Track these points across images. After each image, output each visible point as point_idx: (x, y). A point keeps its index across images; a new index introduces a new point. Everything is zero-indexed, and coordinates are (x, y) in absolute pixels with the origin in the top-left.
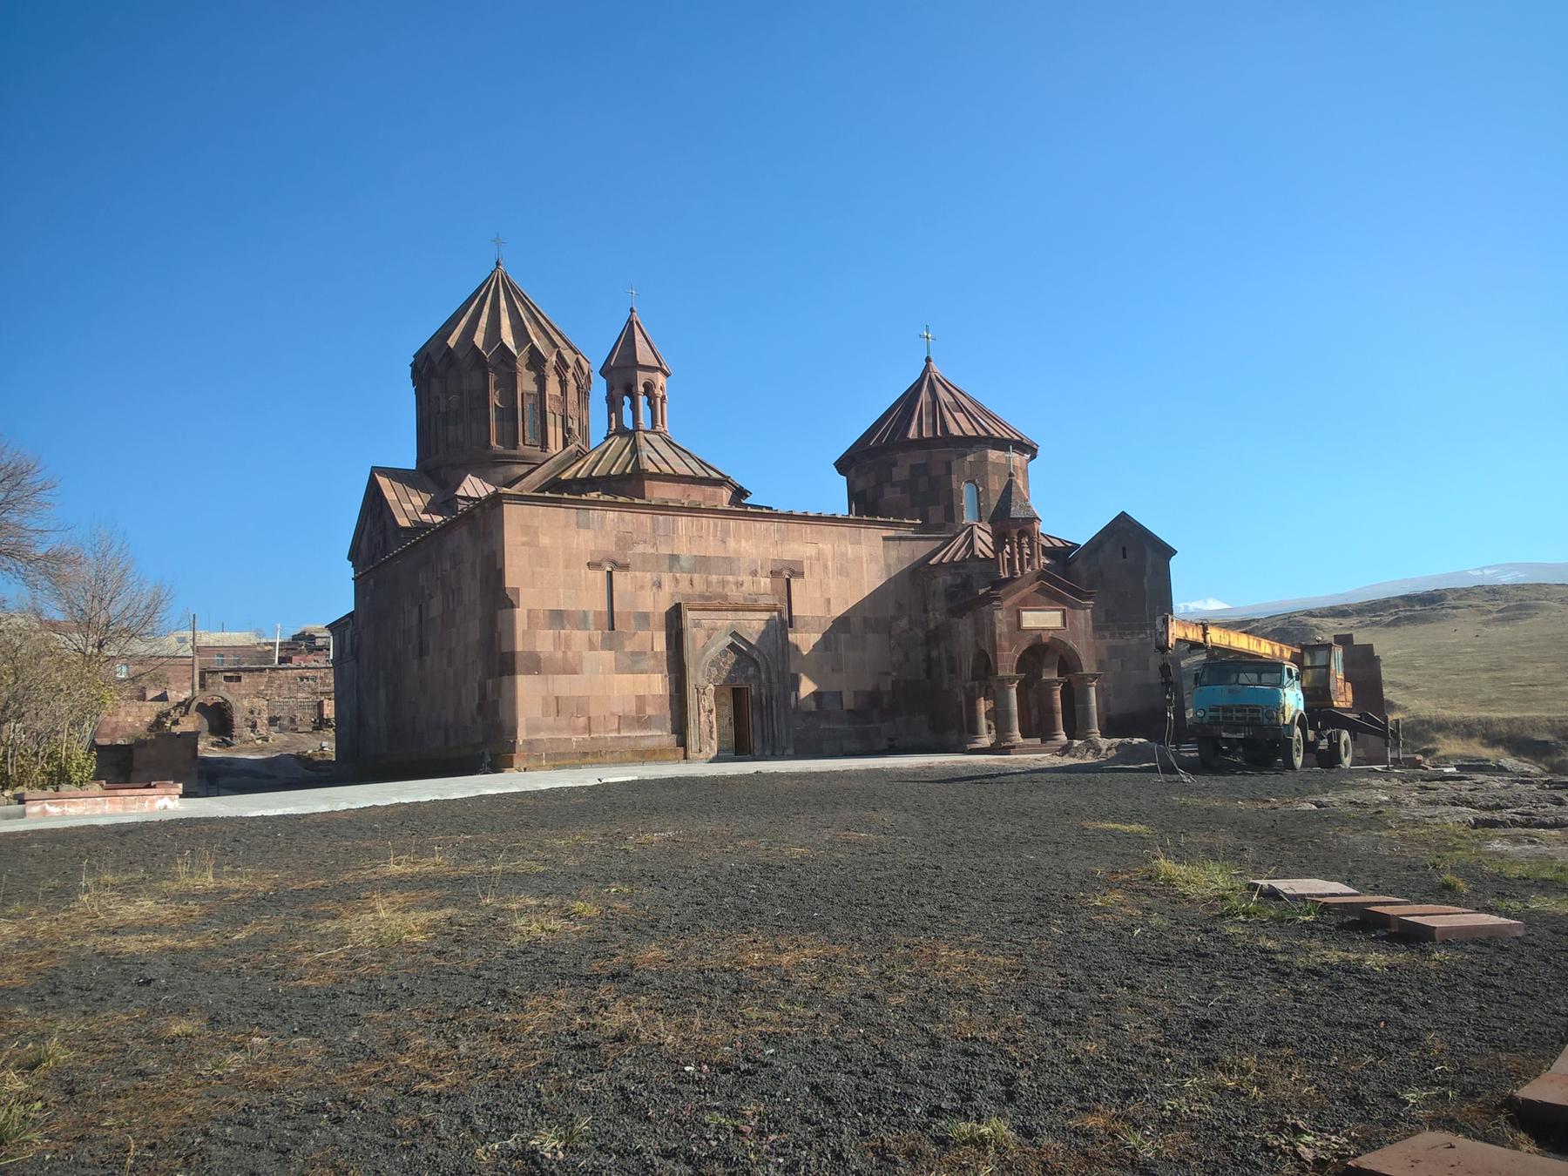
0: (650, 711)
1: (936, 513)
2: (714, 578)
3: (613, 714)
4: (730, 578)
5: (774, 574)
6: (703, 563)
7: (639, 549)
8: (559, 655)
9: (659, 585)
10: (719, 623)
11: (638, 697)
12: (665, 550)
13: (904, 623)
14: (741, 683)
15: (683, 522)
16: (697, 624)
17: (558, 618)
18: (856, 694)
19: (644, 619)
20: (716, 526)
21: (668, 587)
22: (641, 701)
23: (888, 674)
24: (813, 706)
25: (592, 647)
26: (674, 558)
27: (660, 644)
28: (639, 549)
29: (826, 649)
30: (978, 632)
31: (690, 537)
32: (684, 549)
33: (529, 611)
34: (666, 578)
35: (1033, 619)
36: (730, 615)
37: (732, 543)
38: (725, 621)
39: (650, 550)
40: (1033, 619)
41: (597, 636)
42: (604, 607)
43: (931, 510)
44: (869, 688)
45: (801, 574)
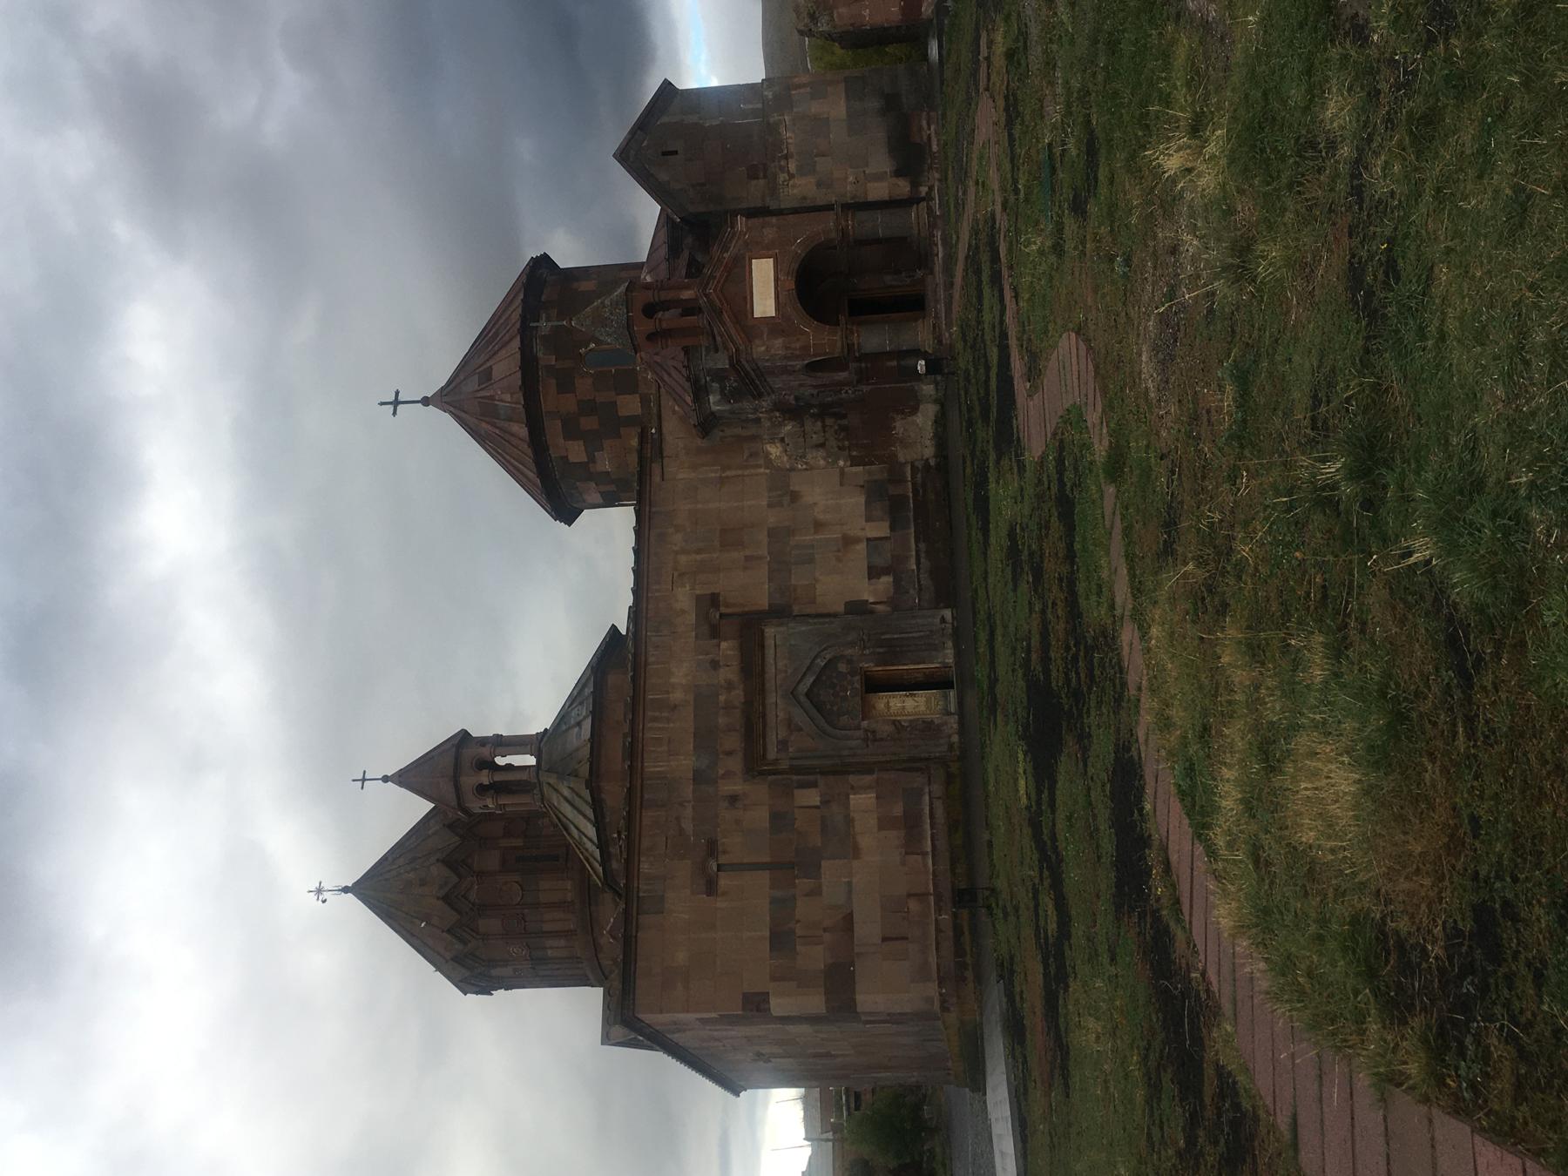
0: (898, 810)
1: (630, 405)
2: (722, 721)
3: (903, 863)
4: (722, 698)
5: (715, 633)
6: (705, 738)
7: (688, 826)
8: (827, 937)
9: (733, 799)
10: (781, 715)
11: (881, 828)
12: (688, 791)
13: (774, 451)
14: (857, 682)
15: (651, 767)
16: (783, 745)
17: (781, 940)
18: (868, 519)
19: (779, 820)
20: (655, 719)
21: (736, 786)
22: (885, 823)
23: (842, 473)
24: (886, 580)
25: (816, 892)
26: (699, 777)
27: (811, 797)
28: (688, 826)
29: (811, 560)
30: (785, 370)
31: (673, 758)
32: (684, 763)
33: (774, 979)
34: (728, 788)
35: (764, 304)
36: (771, 699)
37: (677, 696)
38: (777, 707)
39: (689, 812)
40: (764, 304)
41: (804, 884)
42: (766, 874)
43: (623, 412)
44: (862, 500)
45: (714, 599)
